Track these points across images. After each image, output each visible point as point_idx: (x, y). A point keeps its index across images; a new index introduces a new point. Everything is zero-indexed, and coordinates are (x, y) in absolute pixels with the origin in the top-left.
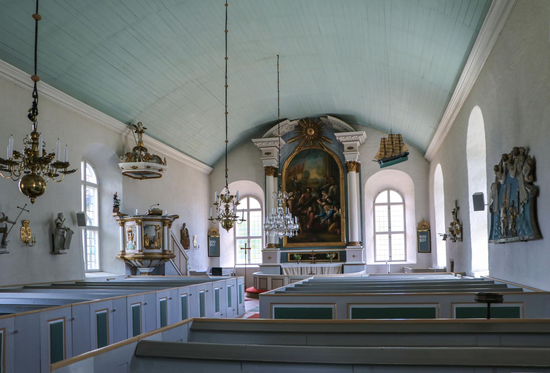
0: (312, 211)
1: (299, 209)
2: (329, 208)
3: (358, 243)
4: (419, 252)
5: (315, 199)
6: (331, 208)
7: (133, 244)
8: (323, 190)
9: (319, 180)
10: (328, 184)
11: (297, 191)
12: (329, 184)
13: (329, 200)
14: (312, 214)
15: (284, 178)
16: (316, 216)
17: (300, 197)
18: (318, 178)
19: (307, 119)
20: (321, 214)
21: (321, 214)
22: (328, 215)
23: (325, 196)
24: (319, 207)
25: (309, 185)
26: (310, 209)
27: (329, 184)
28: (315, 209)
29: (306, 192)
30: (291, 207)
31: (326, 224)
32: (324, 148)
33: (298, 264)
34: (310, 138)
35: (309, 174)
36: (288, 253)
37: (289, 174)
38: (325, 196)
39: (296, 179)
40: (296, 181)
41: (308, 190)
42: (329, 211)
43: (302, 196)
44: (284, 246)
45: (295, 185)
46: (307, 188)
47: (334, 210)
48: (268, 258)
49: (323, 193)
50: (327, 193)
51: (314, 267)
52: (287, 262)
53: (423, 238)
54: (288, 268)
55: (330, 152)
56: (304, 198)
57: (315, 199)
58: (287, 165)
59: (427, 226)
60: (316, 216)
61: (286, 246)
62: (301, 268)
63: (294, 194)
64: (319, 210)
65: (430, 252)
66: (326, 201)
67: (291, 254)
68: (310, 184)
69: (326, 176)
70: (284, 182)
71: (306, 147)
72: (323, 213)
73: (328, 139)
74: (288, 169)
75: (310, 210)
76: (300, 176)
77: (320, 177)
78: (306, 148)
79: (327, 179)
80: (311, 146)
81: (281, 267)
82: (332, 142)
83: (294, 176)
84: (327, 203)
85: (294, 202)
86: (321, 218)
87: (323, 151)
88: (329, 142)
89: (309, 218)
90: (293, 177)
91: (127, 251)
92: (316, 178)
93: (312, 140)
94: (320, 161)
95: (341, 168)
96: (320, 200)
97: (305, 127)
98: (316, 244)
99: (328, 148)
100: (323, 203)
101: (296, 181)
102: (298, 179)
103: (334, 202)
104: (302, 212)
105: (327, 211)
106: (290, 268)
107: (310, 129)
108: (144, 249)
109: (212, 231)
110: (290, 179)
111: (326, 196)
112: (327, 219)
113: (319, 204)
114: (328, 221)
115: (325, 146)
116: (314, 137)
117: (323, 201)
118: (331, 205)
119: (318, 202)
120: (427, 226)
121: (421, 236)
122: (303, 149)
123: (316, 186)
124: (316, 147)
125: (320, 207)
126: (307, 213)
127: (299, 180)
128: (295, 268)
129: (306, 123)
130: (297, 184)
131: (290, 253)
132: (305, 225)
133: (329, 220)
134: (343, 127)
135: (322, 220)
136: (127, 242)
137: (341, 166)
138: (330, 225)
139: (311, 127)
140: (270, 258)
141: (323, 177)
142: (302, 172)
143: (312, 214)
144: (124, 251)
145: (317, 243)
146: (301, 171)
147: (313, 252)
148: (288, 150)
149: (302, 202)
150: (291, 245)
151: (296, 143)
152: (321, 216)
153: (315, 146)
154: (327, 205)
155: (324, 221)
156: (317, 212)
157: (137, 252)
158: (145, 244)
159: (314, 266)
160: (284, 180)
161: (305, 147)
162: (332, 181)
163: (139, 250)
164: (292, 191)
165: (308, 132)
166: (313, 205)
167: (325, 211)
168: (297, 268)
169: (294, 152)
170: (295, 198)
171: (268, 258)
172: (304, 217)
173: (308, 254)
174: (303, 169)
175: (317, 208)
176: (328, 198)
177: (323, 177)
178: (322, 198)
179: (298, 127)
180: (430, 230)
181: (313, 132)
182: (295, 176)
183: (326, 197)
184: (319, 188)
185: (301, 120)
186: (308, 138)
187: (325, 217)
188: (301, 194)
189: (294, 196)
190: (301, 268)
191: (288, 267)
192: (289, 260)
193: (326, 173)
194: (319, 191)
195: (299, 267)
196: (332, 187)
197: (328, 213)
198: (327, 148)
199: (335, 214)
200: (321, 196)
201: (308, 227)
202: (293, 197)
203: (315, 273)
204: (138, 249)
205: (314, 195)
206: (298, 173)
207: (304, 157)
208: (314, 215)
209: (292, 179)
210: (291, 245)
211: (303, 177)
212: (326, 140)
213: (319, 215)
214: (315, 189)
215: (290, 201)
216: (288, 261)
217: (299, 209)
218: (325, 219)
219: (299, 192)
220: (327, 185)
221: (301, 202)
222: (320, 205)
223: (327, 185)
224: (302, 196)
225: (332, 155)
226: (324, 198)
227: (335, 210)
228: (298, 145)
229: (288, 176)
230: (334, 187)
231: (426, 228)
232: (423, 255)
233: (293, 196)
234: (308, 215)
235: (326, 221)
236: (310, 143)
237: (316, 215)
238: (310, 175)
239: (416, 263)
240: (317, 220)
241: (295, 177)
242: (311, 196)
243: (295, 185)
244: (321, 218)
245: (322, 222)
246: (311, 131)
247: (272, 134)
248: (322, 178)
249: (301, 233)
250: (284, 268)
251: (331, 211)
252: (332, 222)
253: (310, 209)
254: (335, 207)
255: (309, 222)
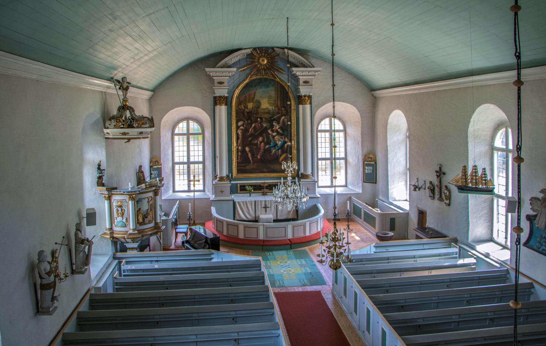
0: (263, 141)
1: (250, 139)
2: (279, 138)
3: (311, 176)
4: (364, 182)
5: (266, 129)
6: (282, 139)
7: (124, 221)
8: (275, 120)
9: (270, 110)
10: (279, 114)
11: (247, 120)
12: (280, 114)
13: (280, 131)
14: (262, 144)
15: (234, 107)
16: (267, 146)
17: (251, 126)
18: (269, 108)
19: (261, 49)
20: (272, 144)
21: (272, 144)
22: (279, 146)
23: (277, 127)
24: (270, 137)
25: (260, 115)
26: (261, 139)
27: (280, 114)
28: (266, 139)
29: (256, 121)
30: (241, 137)
31: (277, 154)
32: (276, 78)
33: (250, 196)
34: (262, 67)
35: (260, 104)
36: (238, 184)
37: (239, 103)
38: (277, 127)
39: (247, 108)
40: (246, 110)
41: (259, 119)
42: (280, 142)
43: (253, 125)
44: (233, 177)
45: (246, 114)
46: (258, 118)
47: (285, 141)
48: (221, 192)
49: (274, 124)
50: (278, 123)
51: (269, 201)
52: (237, 193)
53: (369, 170)
54: (242, 201)
55: (282, 82)
56: (255, 127)
57: (266, 129)
58: (237, 94)
59: (373, 159)
60: (267, 146)
61: (236, 177)
62: (255, 201)
63: (245, 123)
64: (271, 141)
65: (376, 183)
66: (277, 131)
67: (241, 185)
68: (262, 114)
69: (277, 106)
70: (234, 110)
71: (258, 76)
72: (274, 143)
73: (281, 69)
74: (238, 97)
75: (261, 140)
76: (250, 106)
77: (271, 107)
78: (257, 77)
79: (279, 109)
80: (263, 75)
81: (235, 201)
82: (285, 73)
83: (245, 105)
84: (278, 133)
85: (245, 131)
86: (272, 148)
87: (275, 81)
88: (281, 73)
89: (260, 149)
90: (244, 106)
91: (115, 229)
92: (268, 108)
93: (264, 69)
94: (272, 91)
95: (293, 99)
96: (271, 131)
97: (258, 56)
98: (267, 175)
99: (280, 79)
100: (275, 134)
101: (246, 110)
102: (248, 108)
103: (285, 133)
104: (253, 142)
105: (278, 141)
106: (244, 201)
107: (263, 58)
108: (138, 225)
109: (154, 161)
110: (240, 107)
111: (277, 126)
112: (278, 150)
113: (270, 134)
114: (278, 152)
115: (277, 77)
116: (266, 66)
117: (274, 131)
118: (282, 136)
119: (269, 132)
120: (373, 159)
121: (366, 167)
122: (254, 77)
123: (267, 116)
124: (268, 77)
125: (271, 138)
126: (257, 143)
127: (251, 109)
128: (249, 201)
129: (259, 52)
130: (248, 113)
131: (240, 183)
132: (255, 156)
133: (280, 150)
134: (299, 61)
135: (273, 150)
136: (115, 219)
137: (293, 97)
138: (281, 156)
139: (264, 56)
140: (222, 192)
141: (275, 107)
142: (252, 102)
143: (262, 144)
144: (111, 229)
145: (268, 174)
146: (252, 100)
147: (264, 183)
148: (238, 78)
149: (252, 131)
150: (241, 176)
151: (248, 71)
152: (272, 147)
153: (266, 75)
154: (278, 136)
155: (275, 152)
156: (268, 143)
157: (131, 231)
158: (138, 220)
159: (268, 200)
160: (234, 109)
161: (256, 76)
162: (284, 112)
163: (133, 229)
164: (242, 120)
165: (260, 60)
166: (264, 135)
167: (276, 141)
168: (251, 201)
169: (244, 80)
170: (246, 128)
171: (221, 192)
172: (255, 147)
173: (258, 185)
174: (254, 98)
175: (268, 138)
176: (279, 128)
177: (274, 107)
178: (273, 129)
179: (250, 56)
180: (376, 163)
181: (266, 62)
182: (246, 105)
183: (278, 127)
184: (271, 118)
185: (255, 49)
186: (260, 66)
187: (276, 147)
188: (251, 124)
189: (245, 126)
190: (255, 201)
191: (242, 201)
192: (239, 191)
193: (278, 103)
194: (270, 121)
195: (253, 201)
196: (283, 118)
197: (279, 143)
198: (279, 79)
199: (286, 145)
200: (272, 126)
201: (259, 157)
202: (243, 127)
203: (269, 206)
204: (131, 227)
205: (265, 125)
206: (249, 102)
207: (256, 86)
208: (265, 146)
209: (243, 108)
210: (242, 176)
211: (254, 106)
212: (279, 70)
213: (270, 146)
214: (266, 118)
215: (240, 131)
216: (238, 192)
217: (250, 139)
218: (276, 149)
219: (249, 121)
220: (279, 115)
221: (251, 131)
222: (271, 136)
223: (279, 115)
224: (253, 125)
225: (284, 86)
226: (275, 128)
227: (286, 141)
228: (250, 74)
229: (238, 105)
230: (285, 118)
231: (372, 160)
232: (368, 186)
233: (243, 125)
234: (258, 146)
235: (277, 151)
236: (263, 72)
237: (267, 145)
238: (262, 105)
239: (361, 192)
240: (268, 151)
241: (246, 106)
242: (262, 126)
243: (246, 114)
244: (272, 148)
245: (273, 153)
246: (263, 61)
247: (226, 63)
248: (274, 108)
249: (252, 163)
250: (238, 202)
251: (282, 142)
252: (283, 152)
253: (261, 139)
254: (286, 138)
255: (260, 153)
